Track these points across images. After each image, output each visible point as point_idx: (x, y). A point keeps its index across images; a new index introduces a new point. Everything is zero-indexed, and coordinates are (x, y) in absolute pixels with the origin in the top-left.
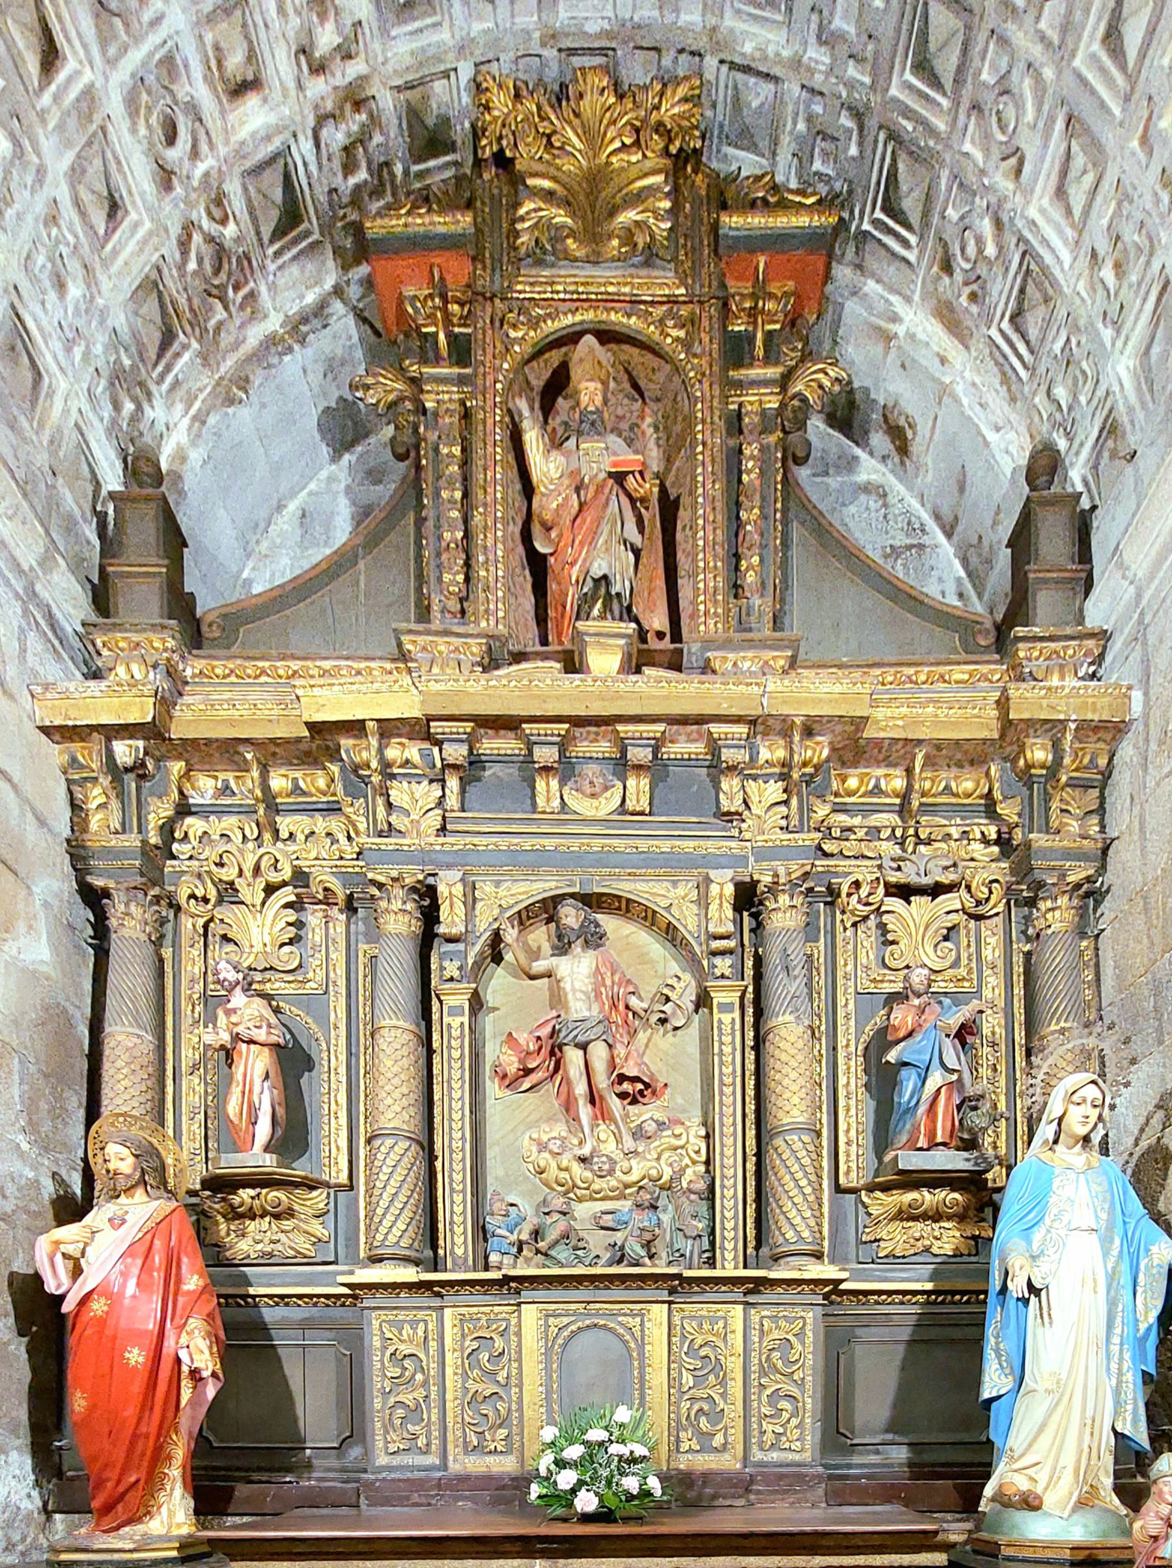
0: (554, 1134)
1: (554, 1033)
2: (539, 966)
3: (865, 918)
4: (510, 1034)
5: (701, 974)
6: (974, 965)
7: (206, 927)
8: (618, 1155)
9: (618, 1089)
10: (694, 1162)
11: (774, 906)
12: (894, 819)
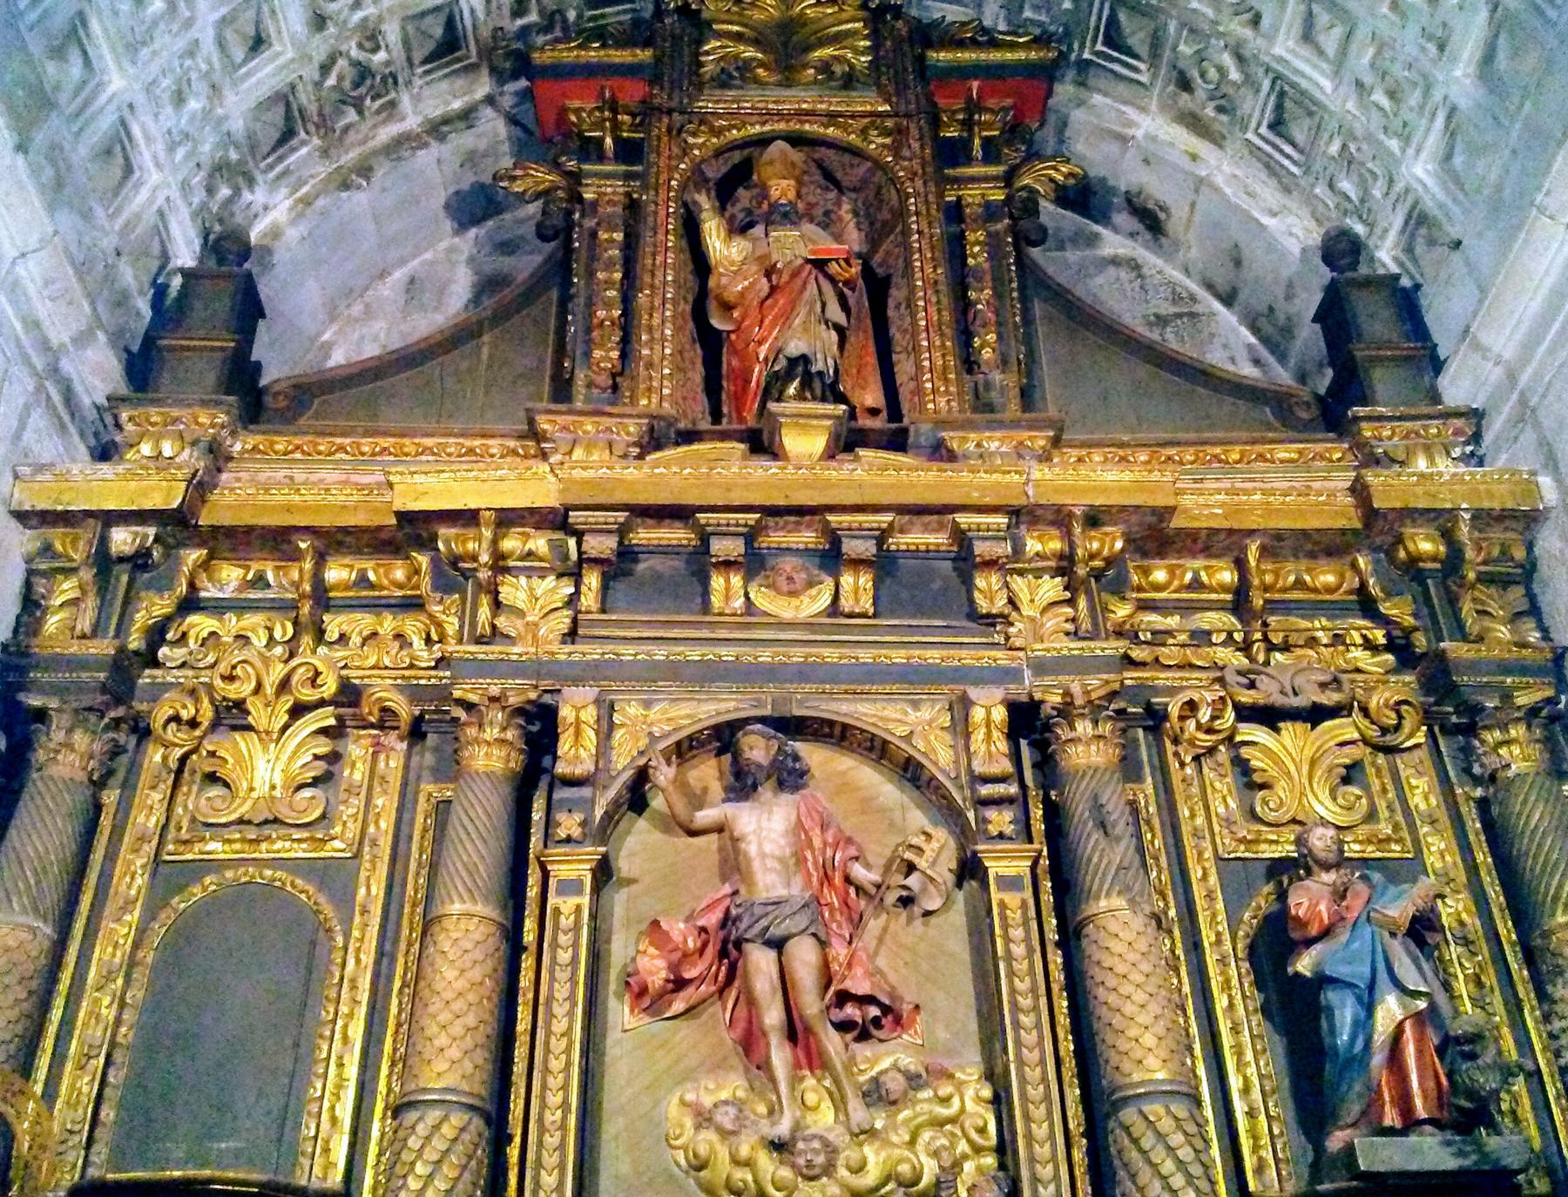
0: (724, 1095)
1: (727, 920)
2: (705, 816)
3: (1211, 751)
4: (655, 924)
5: (963, 834)
6: (1400, 818)
7: (183, 760)
8: (838, 1136)
9: (837, 1015)
11: (1071, 735)
12: (1229, 620)
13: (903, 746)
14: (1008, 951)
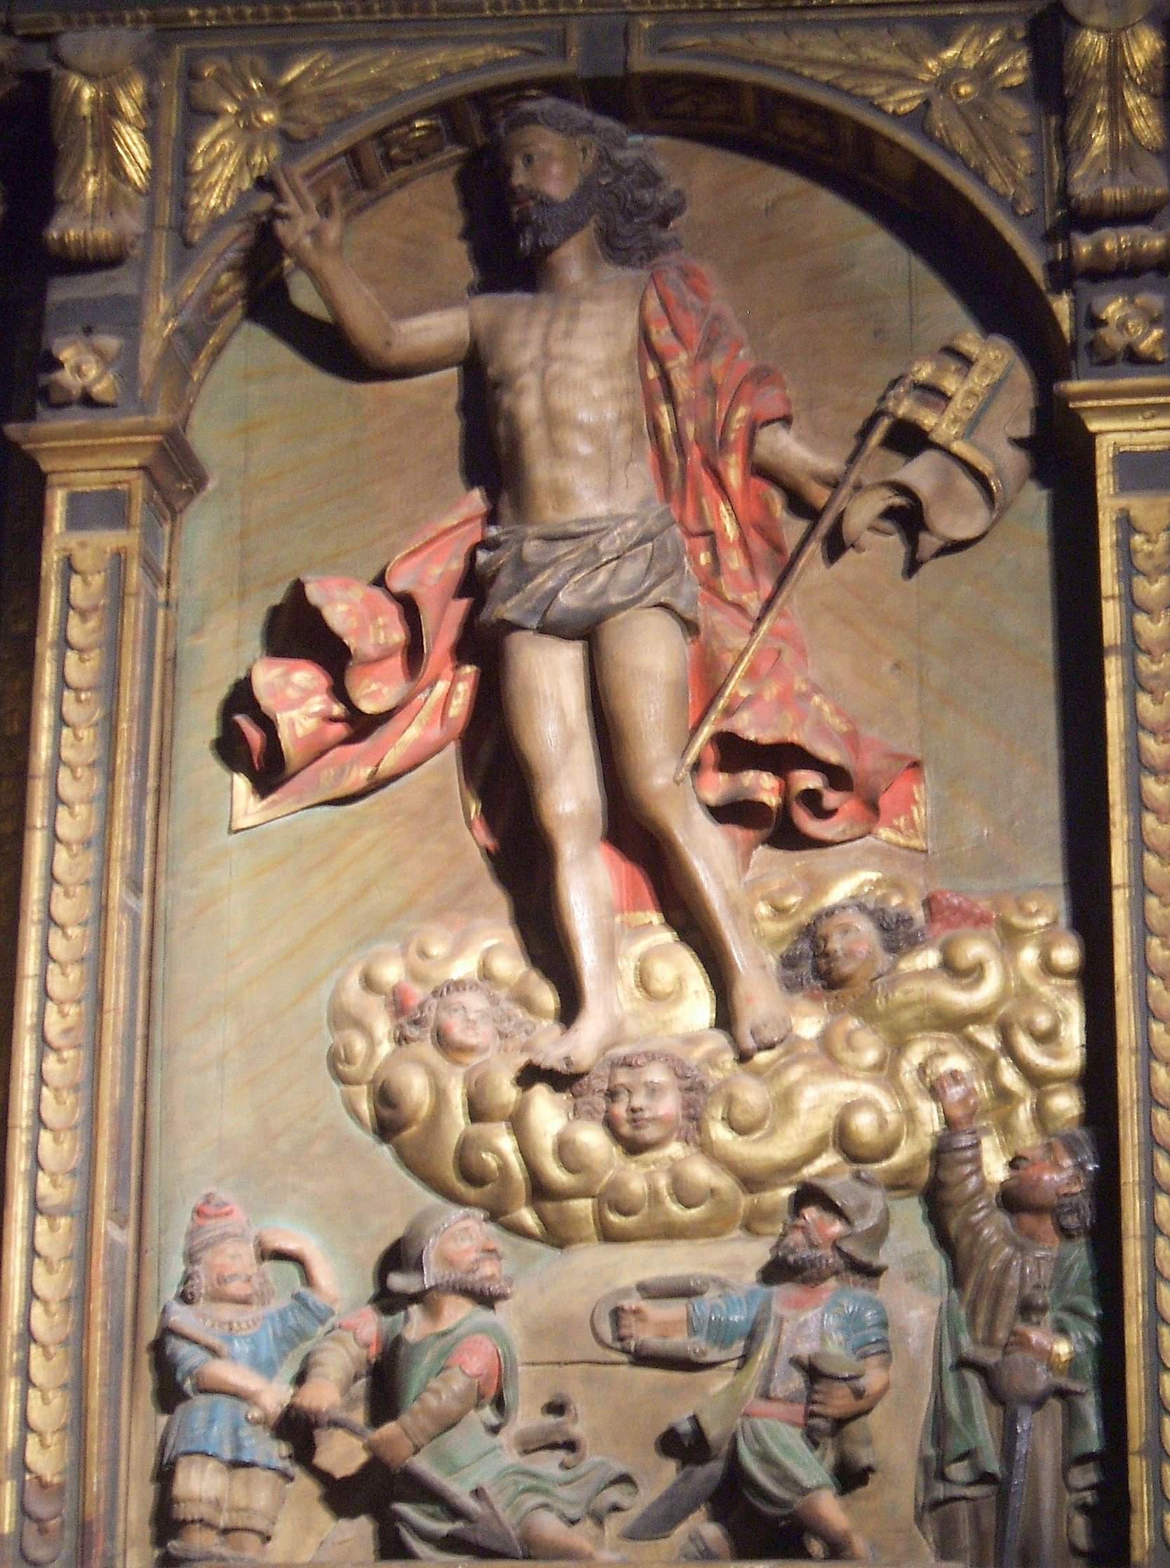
10: (1035, 1079)
13: (905, 138)
14: (1131, 633)
